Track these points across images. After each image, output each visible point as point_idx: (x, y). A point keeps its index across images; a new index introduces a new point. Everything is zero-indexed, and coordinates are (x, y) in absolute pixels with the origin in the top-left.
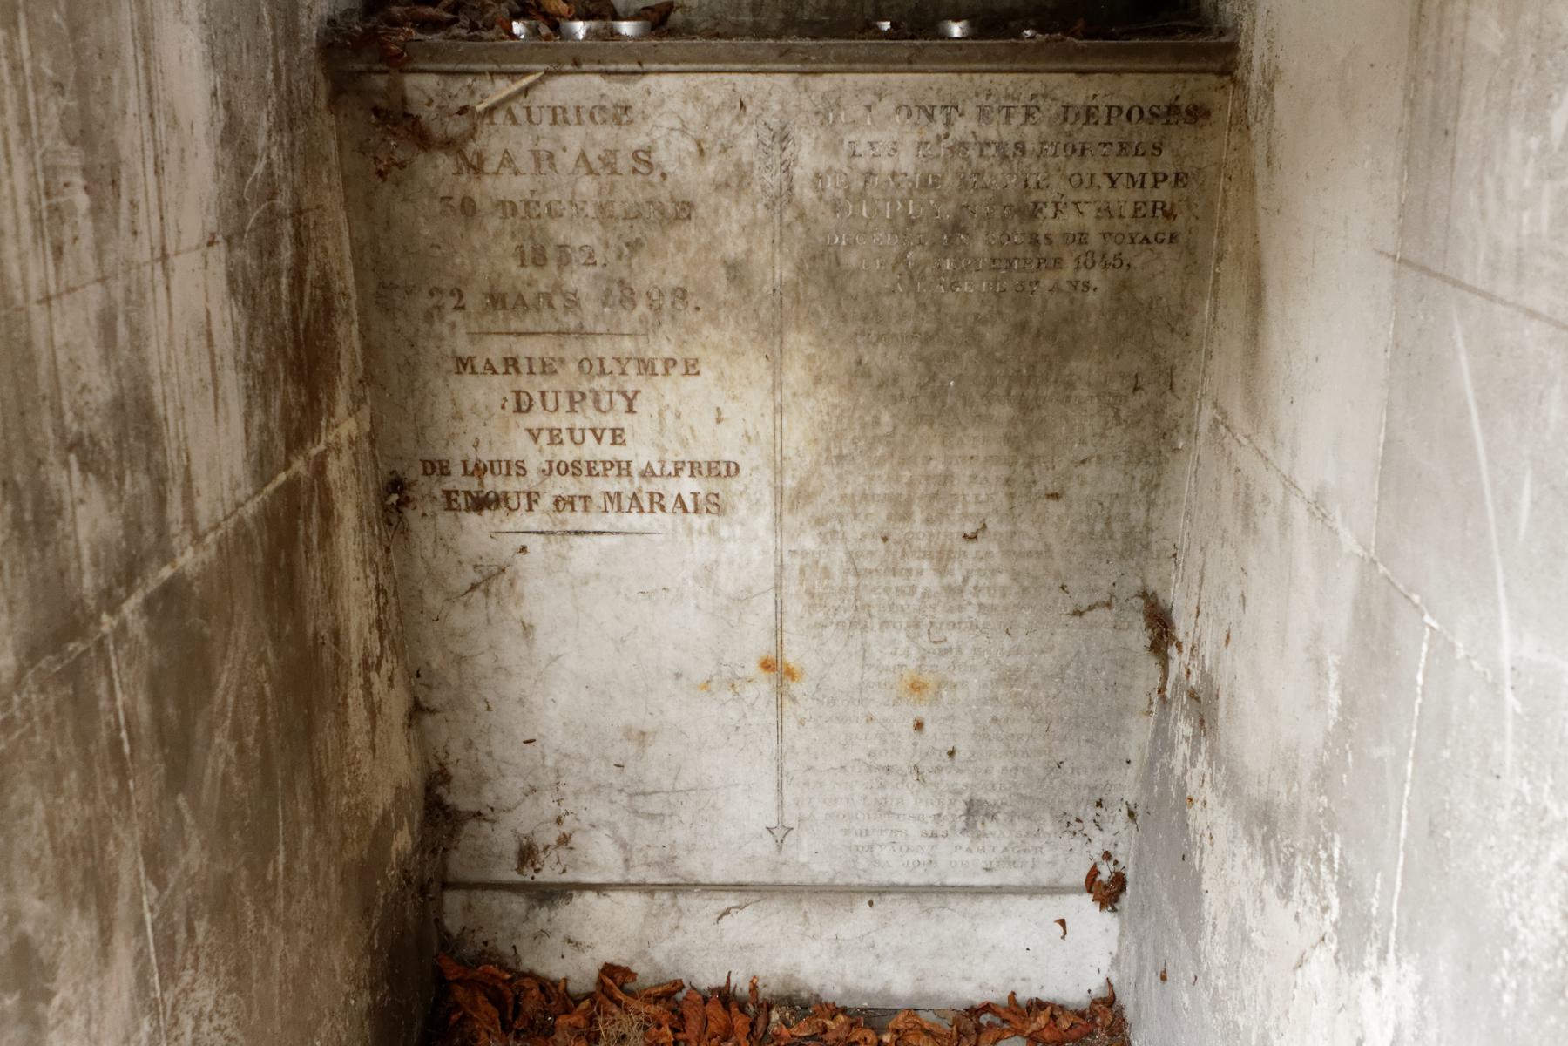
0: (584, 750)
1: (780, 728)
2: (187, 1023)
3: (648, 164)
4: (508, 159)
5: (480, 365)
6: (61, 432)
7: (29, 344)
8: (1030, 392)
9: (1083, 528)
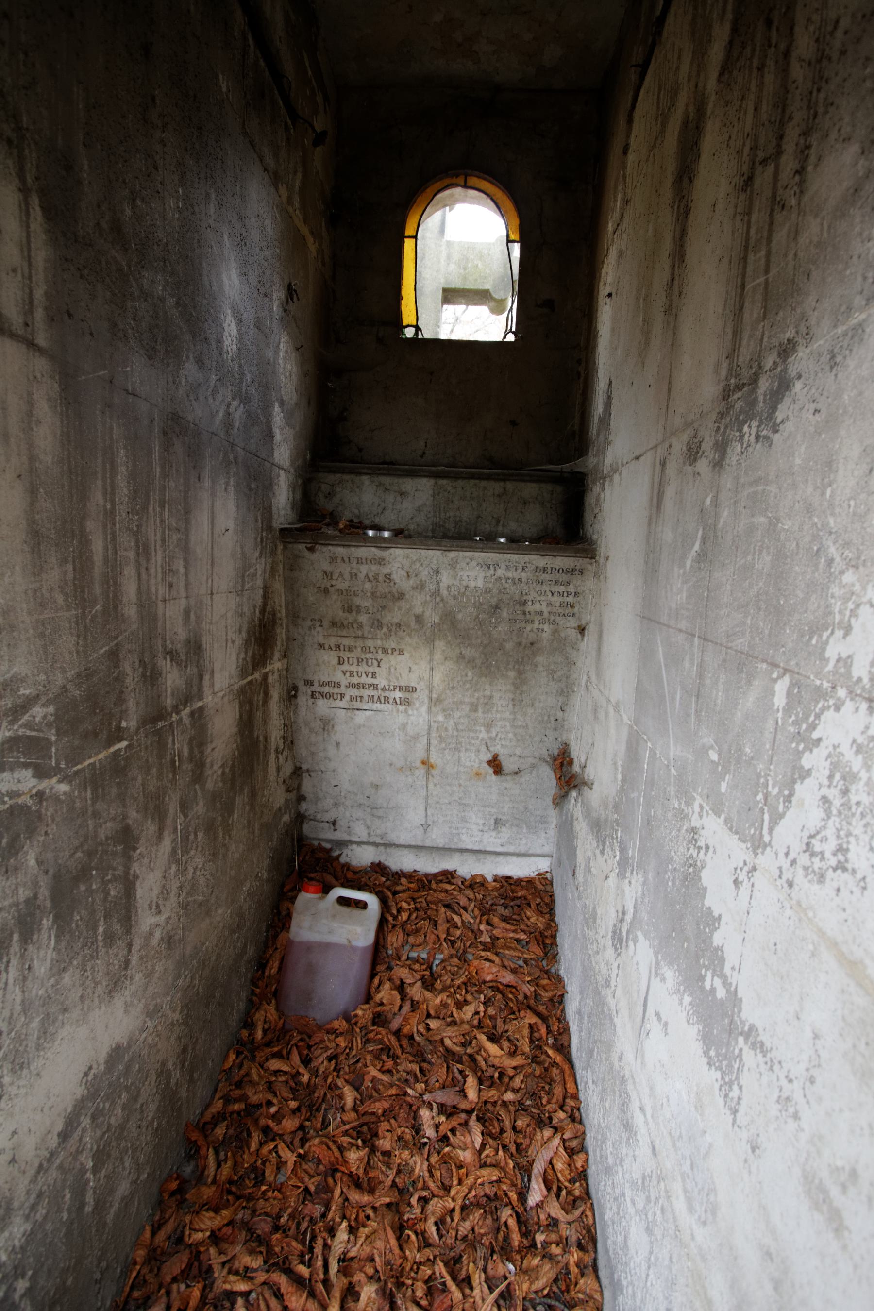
0: (356, 791)
1: (427, 787)
2: (191, 870)
3: (390, 579)
4: (341, 575)
5: (327, 647)
6: (164, 646)
7: (156, 614)
8: (522, 667)
9: (540, 718)
